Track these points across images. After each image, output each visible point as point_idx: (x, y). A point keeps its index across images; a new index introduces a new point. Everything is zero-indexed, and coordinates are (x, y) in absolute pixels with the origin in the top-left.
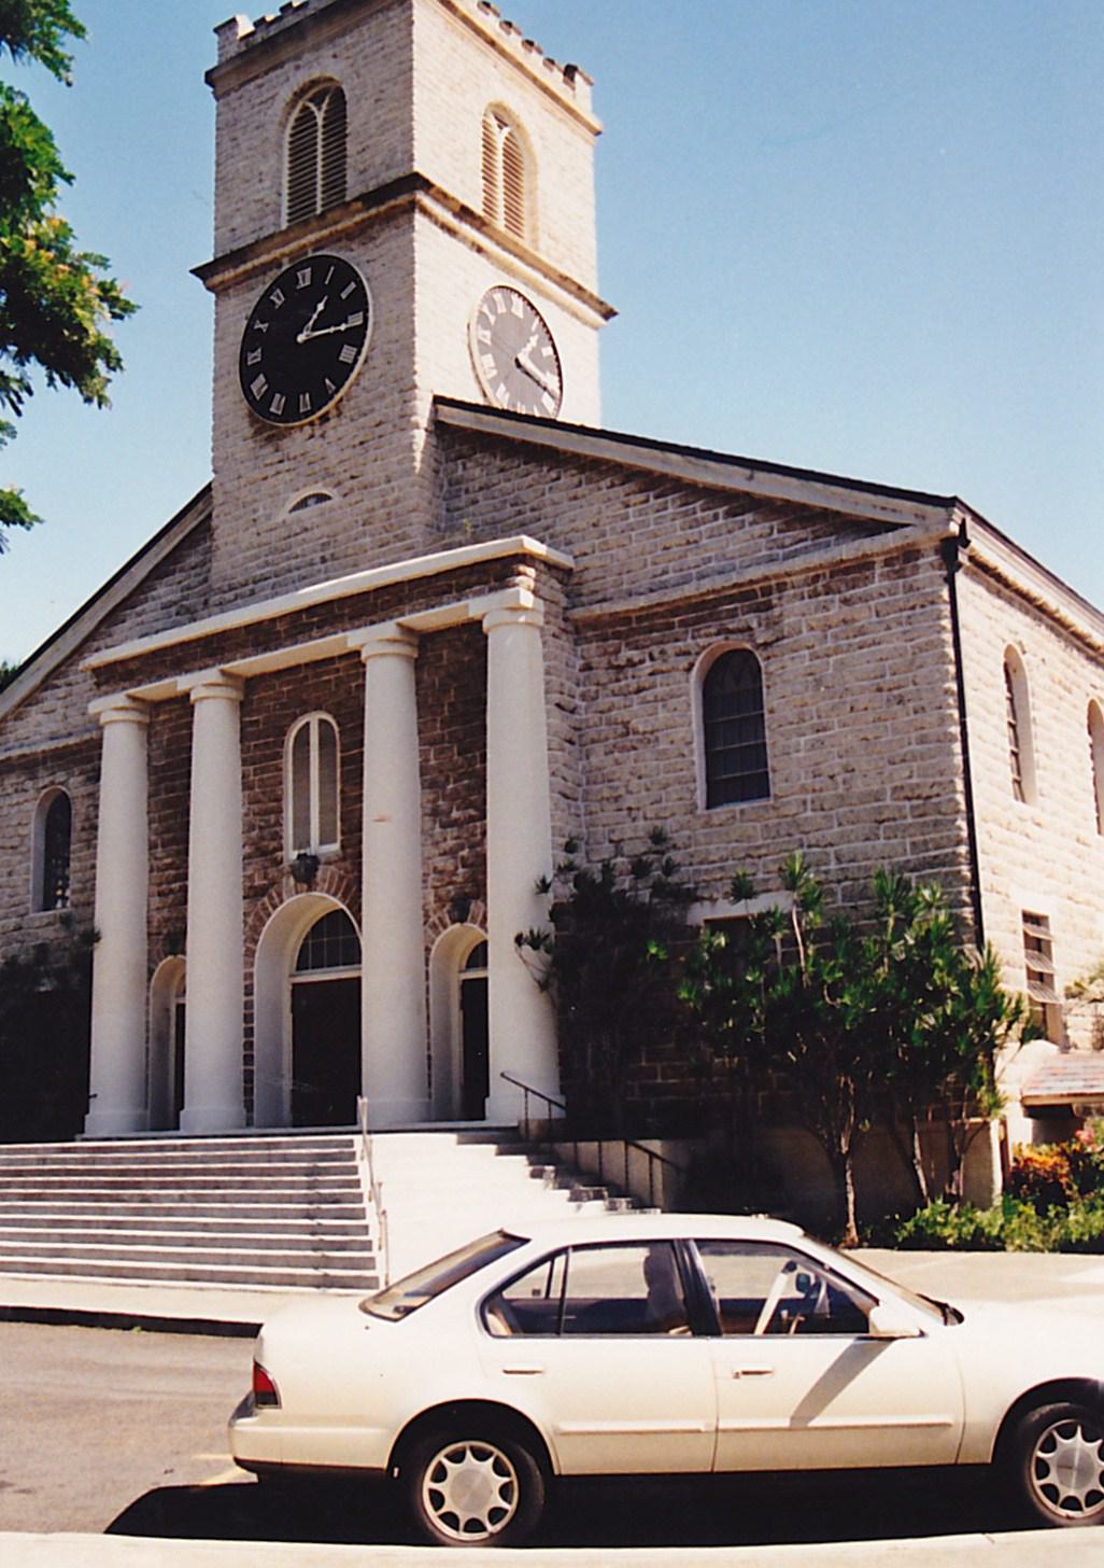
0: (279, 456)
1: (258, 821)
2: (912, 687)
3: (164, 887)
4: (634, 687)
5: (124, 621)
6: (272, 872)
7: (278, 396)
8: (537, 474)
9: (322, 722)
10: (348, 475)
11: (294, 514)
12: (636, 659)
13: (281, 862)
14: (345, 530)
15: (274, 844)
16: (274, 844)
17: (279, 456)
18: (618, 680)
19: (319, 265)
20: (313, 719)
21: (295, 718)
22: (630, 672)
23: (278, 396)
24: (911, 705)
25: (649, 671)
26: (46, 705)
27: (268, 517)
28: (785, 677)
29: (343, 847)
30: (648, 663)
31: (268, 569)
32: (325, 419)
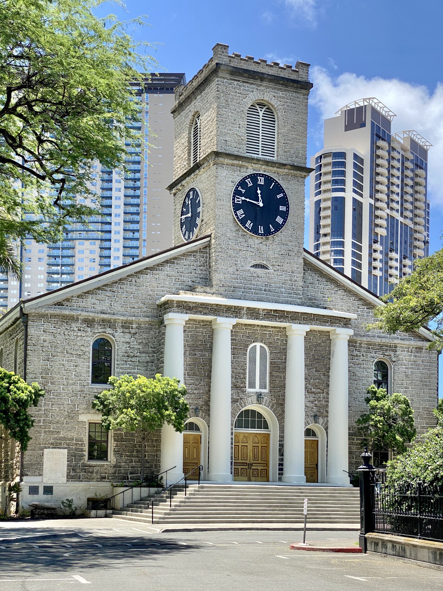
2: (428, 383)
3: (190, 391)
4: (358, 363)
7: (249, 222)
8: (330, 286)
9: (261, 347)
10: (277, 264)
11: (253, 269)
12: (359, 355)
18: (353, 359)
19: (269, 180)
20: (258, 345)
22: (356, 358)
23: (249, 222)
24: (428, 387)
25: (362, 359)
26: (99, 297)
28: (399, 372)
29: (270, 392)
30: (362, 357)
31: (241, 285)
32: (267, 239)
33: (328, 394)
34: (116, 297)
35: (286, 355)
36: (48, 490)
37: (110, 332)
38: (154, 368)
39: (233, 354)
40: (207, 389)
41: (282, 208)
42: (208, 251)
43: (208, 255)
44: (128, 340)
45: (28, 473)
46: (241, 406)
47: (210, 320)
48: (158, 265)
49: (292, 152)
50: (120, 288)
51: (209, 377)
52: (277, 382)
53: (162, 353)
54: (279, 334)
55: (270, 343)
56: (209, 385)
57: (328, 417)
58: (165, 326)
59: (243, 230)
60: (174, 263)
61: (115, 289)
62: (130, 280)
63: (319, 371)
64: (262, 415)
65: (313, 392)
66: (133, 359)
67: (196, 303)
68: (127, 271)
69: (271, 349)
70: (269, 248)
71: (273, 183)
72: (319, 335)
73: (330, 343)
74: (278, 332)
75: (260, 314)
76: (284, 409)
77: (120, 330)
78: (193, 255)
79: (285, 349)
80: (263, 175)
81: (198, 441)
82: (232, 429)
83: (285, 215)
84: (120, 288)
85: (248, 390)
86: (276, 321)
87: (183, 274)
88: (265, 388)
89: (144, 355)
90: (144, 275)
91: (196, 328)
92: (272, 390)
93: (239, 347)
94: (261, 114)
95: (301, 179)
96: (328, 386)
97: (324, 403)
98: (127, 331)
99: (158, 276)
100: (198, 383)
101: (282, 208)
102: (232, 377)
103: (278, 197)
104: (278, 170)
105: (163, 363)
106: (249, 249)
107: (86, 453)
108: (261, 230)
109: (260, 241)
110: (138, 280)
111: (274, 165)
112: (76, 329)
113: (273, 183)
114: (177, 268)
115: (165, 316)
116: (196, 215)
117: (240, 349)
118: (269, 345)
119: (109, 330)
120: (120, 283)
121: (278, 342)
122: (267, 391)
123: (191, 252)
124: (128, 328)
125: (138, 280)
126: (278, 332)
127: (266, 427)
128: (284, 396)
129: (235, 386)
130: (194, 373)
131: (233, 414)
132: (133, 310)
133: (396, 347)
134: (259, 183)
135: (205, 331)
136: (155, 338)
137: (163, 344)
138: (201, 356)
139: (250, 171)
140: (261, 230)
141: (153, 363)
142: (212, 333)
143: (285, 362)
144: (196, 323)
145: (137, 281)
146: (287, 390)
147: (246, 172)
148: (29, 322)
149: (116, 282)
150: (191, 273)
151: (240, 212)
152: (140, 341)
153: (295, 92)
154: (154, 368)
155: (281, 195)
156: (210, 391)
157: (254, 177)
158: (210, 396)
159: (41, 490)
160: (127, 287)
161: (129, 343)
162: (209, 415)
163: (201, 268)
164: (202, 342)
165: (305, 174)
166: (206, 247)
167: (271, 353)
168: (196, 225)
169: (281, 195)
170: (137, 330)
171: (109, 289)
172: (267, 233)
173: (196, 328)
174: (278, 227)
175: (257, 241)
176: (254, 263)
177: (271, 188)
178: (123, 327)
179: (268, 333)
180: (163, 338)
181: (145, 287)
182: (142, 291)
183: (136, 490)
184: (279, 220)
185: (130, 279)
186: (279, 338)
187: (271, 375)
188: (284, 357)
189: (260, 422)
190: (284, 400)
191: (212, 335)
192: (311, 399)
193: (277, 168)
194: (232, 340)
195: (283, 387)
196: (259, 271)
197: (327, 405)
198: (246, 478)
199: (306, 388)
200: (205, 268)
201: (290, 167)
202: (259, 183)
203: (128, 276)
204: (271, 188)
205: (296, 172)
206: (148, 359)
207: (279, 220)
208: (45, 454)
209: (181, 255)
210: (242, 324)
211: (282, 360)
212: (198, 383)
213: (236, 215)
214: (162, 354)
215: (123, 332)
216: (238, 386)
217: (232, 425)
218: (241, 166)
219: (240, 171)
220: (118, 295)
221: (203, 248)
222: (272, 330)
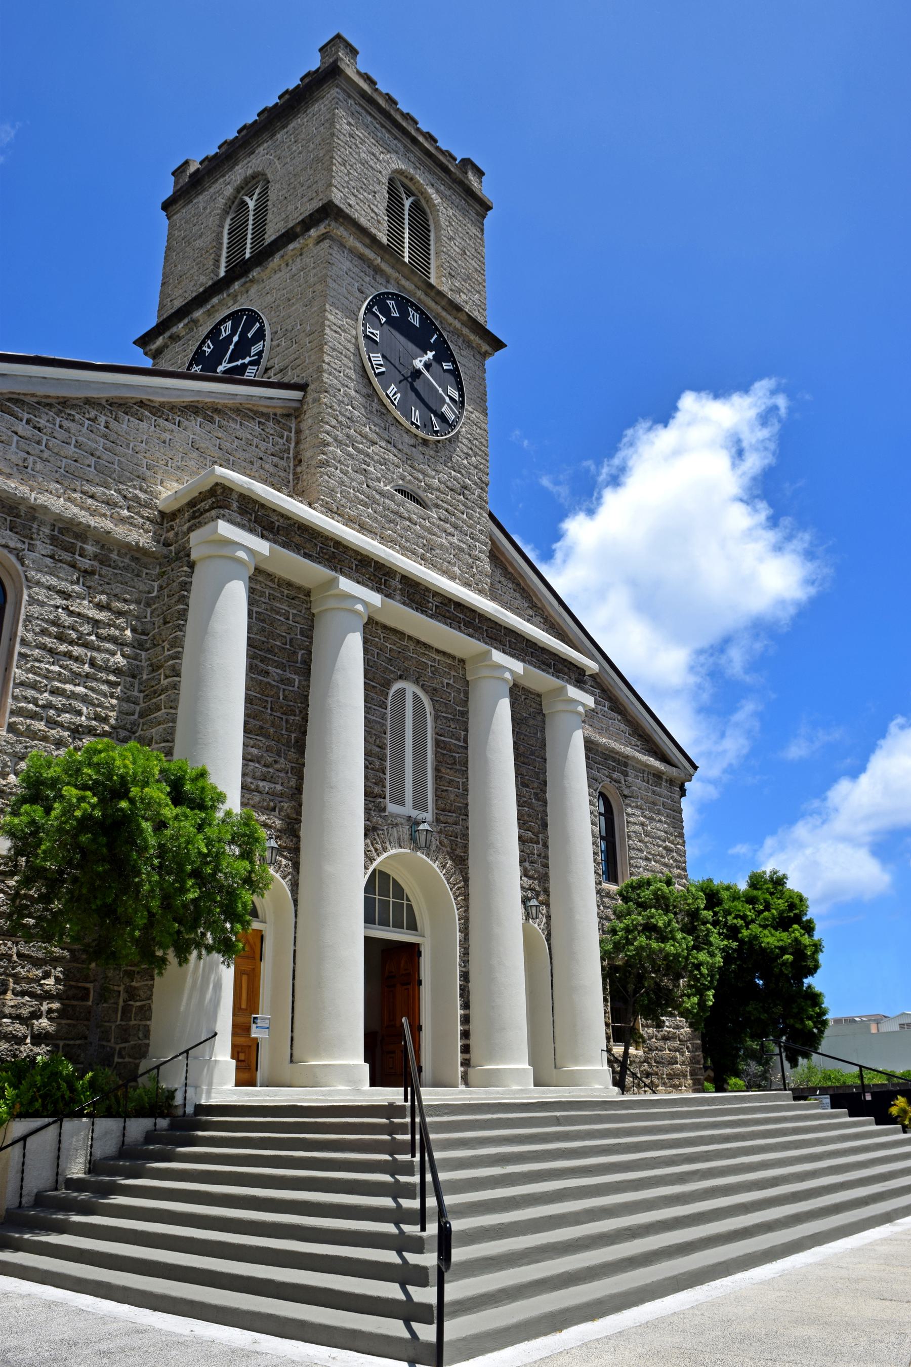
5: (142, 421)
13: (384, 810)
15: (377, 790)
20: (410, 688)
34: (43, 448)
35: (466, 730)
37: (12, 544)
38: (136, 693)
42: (293, 426)
43: (293, 435)
46: (376, 850)
47: (306, 584)
48: (173, 408)
50: (61, 427)
51: (300, 747)
52: (452, 797)
54: (453, 673)
55: (435, 690)
56: (298, 772)
58: (192, 565)
59: (380, 400)
60: (212, 421)
61: (42, 422)
62: (92, 415)
63: (528, 786)
64: (402, 890)
67: (288, 518)
68: (88, 383)
69: (437, 706)
71: (435, 336)
72: (523, 697)
73: (544, 722)
75: (429, 602)
76: (467, 874)
77: (43, 548)
78: (259, 422)
79: (464, 714)
84: (61, 427)
86: (461, 631)
87: (232, 458)
90: (132, 419)
91: (272, 597)
92: (442, 818)
94: (407, 203)
98: (66, 556)
99: (169, 437)
100: (270, 760)
104: (444, 314)
105: (178, 675)
109: (412, 441)
110: (113, 424)
111: (438, 298)
113: (435, 336)
114: (220, 435)
115: (192, 535)
117: (374, 687)
118: (432, 693)
120: (61, 411)
121: (450, 693)
122: (429, 816)
123: (256, 413)
124: (70, 549)
125: (113, 424)
126: (451, 667)
128: (465, 836)
130: (261, 728)
133: (626, 765)
135: (294, 615)
136: (148, 605)
138: (282, 681)
141: (134, 677)
142: (309, 623)
143: (466, 748)
144: (270, 584)
145: (111, 426)
146: (471, 822)
147: (386, 288)
149: (50, 405)
150: (252, 463)
153: (465, 200)
154: (136, 693)
156: (299, 790)
158: (300, 805)
160: (79, 430)
163: (276, 459)
164: (284, 641)
166: (288, 416)
167: (437, 718)
170: (96, 563)
171: (26, 416)
173: (272, 597)
177: (432, 341)
178: (53, 540)
179: (430, 663)
180: (184, 600)
181: (130, 451)
182: (122, 459)
186: (451, 682)
187: (438, 778)
188: (463, 733)
190: (466, 847)
191: (312, 628)
193: (443, 308)
195: (464, 811)
196: (411, 505)
200: (283, 463)
201: (465, 318)
203: (88, 401)
204: (432, 341)
205: (472, 337)
209: (231, 409)
210: (377, 623)
211: (460, 741)
212: (270, 760)
214: (172, 646)
215: (52, 557)
219: (374, 279)
220: (50, 444)
221: (283, 416)
222: (437, 658)
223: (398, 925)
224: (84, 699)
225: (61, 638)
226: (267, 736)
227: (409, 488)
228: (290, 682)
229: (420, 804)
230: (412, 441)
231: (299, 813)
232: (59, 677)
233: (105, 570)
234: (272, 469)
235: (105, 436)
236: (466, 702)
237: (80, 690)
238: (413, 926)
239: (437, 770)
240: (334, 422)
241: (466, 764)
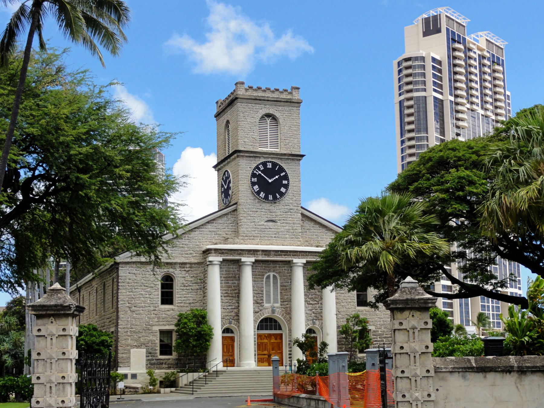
0: (261, 207)
1: (255, 295)
6: (261, 308)
7: (262, 193)
11: (265, 223)
14: (281, 232)
15: (261, 301)
16: (261, 301)
17: (261, 207)
19: (274, 165)
20: (272, 274)
21: (266, 273)
23: (262, 193)
27: (259, 222)
29: (281, 305)
32: (275, 203)
33: (321, 304)
36: (134, 376)
39: (254, 281)
40: (237, 305)
41: (285, 182)
44: (184, 276)
45: (121, 365)
49: (290, 144)
53: (206, 283)
57: (322, 320)
60: (213, 223)
65: (311, 304)
66: (188, 288)
70: (277, 209)
74: (285, 264)
80: (270, 162)
81: (232, 339)
82: (255, 332)
83: (286, 186)
85: (266, 305)
88: (277, 303)
89: (195, 285)
93: (256, 277)
95: (297, 162)
96: (322, 299)
97: (319, 311)
98: (183, 269)
101: (285, 182)
102: (254, 297)
103: (282, 175)
106: (263, 210)
107: (158, 352)
108: (271, 197)
112: (149, 270)
116: (229, 188)
119: (171, 270)
122: (278, 305)
124: (184, 268)
127: (280, 328)
128: (290, 308)
129: (256, 302)
131: (255, 321)
132: (186, 255)
134: (268, 167)
137: (207, 277)
139: (262, 160)
140: (271, 197)
148: (120, 268)
151: (256, 187)
152: (192, 275)
155: (284, 173)
156: (239, 306)
157: (264, 164)
159: (129, 376)
161: (184, 277)
162: (239, 323)
165: (300, 158)
168: (229, 195)
169: (284, 173)
170: (189, 269)
172: (275, 198)
174: (282, 194)
175: (268, 205)
176: (267, 219)
183: (190, 374)
184: (283, 190)
185: (184, 235)
189: (275, 326)
190: (291, 311)
192: (310, 308)
194: (252, 271)
195: (290, 301)
197: (322, 312)
198: (267, 364)
199: (306, 301)
200: (234, 224)
202: (268, 167)
206: (197, 287)
207: (283, 190)
208: (131, 352)
213: (253, 189)
216: (258, 302)
217: (254, 329)
218: (256, 157)
223: (275, 329)
224: (191, 297)
225: (184, 286)
226: (230, 297)
227: (270, 219)
228: (235, 283)
229: (276, 301)
230: (270, 204)
231: (239, 311)
232: (185, 294)
233: (192, 269)
234: (231, 227)
235: (188, 239)
236: (291, 273)
237: (190, 295)
238: (280, 328)
239: (281, 293)
240: (243, 212)
241: (291, 289)
